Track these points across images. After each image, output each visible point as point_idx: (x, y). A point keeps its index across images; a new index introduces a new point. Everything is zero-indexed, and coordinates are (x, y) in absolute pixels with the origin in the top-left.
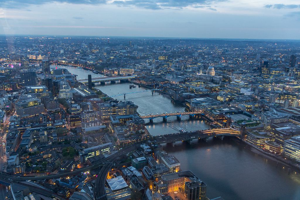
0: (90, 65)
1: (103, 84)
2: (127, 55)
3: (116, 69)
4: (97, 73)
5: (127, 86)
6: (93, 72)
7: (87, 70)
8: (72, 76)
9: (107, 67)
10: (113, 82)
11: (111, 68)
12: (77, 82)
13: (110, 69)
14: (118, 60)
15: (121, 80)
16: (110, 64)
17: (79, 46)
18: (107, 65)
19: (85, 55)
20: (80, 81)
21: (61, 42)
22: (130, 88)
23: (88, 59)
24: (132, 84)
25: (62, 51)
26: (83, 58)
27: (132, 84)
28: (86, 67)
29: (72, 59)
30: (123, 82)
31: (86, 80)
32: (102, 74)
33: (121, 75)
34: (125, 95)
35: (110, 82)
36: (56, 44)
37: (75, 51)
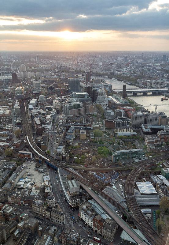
0: (124, 77)
1: (135, 94)
2: (160, 68)
3: (148, 81)
4: (130, 85)
5: (160, 98)
6: (127, 83)
7: (122, 81)
8: (108, 85)
9: (140, 79)
10: (145, 94)
11: (144, 80)
12: (112, 91)
13: (143, 81)
14: (151, 73)
15: (153, 92)
16: (143, 77)
17: (115, 60)
18: (140, 77)
19: (121, 68)
20: (114, 91)
21: (100, 56)
22: (162, 100)
23: (123, 71)
24: (164, 97)
25: (101, 64)
26: (118, 70)
27: (164, 97)
28: (120, 78)
29: (109, 70)
30: (155, 94)
31: (120, 89)
32: (135, 85)
33: (153, 88)
34: (156, 106)
35: (142, 94)
36: (96, 58)
37: (112, 64)
